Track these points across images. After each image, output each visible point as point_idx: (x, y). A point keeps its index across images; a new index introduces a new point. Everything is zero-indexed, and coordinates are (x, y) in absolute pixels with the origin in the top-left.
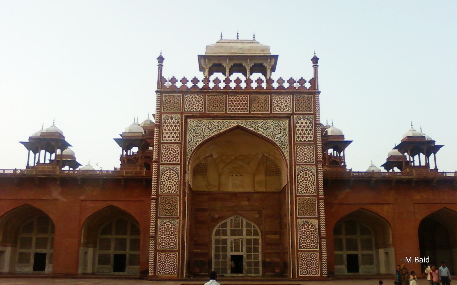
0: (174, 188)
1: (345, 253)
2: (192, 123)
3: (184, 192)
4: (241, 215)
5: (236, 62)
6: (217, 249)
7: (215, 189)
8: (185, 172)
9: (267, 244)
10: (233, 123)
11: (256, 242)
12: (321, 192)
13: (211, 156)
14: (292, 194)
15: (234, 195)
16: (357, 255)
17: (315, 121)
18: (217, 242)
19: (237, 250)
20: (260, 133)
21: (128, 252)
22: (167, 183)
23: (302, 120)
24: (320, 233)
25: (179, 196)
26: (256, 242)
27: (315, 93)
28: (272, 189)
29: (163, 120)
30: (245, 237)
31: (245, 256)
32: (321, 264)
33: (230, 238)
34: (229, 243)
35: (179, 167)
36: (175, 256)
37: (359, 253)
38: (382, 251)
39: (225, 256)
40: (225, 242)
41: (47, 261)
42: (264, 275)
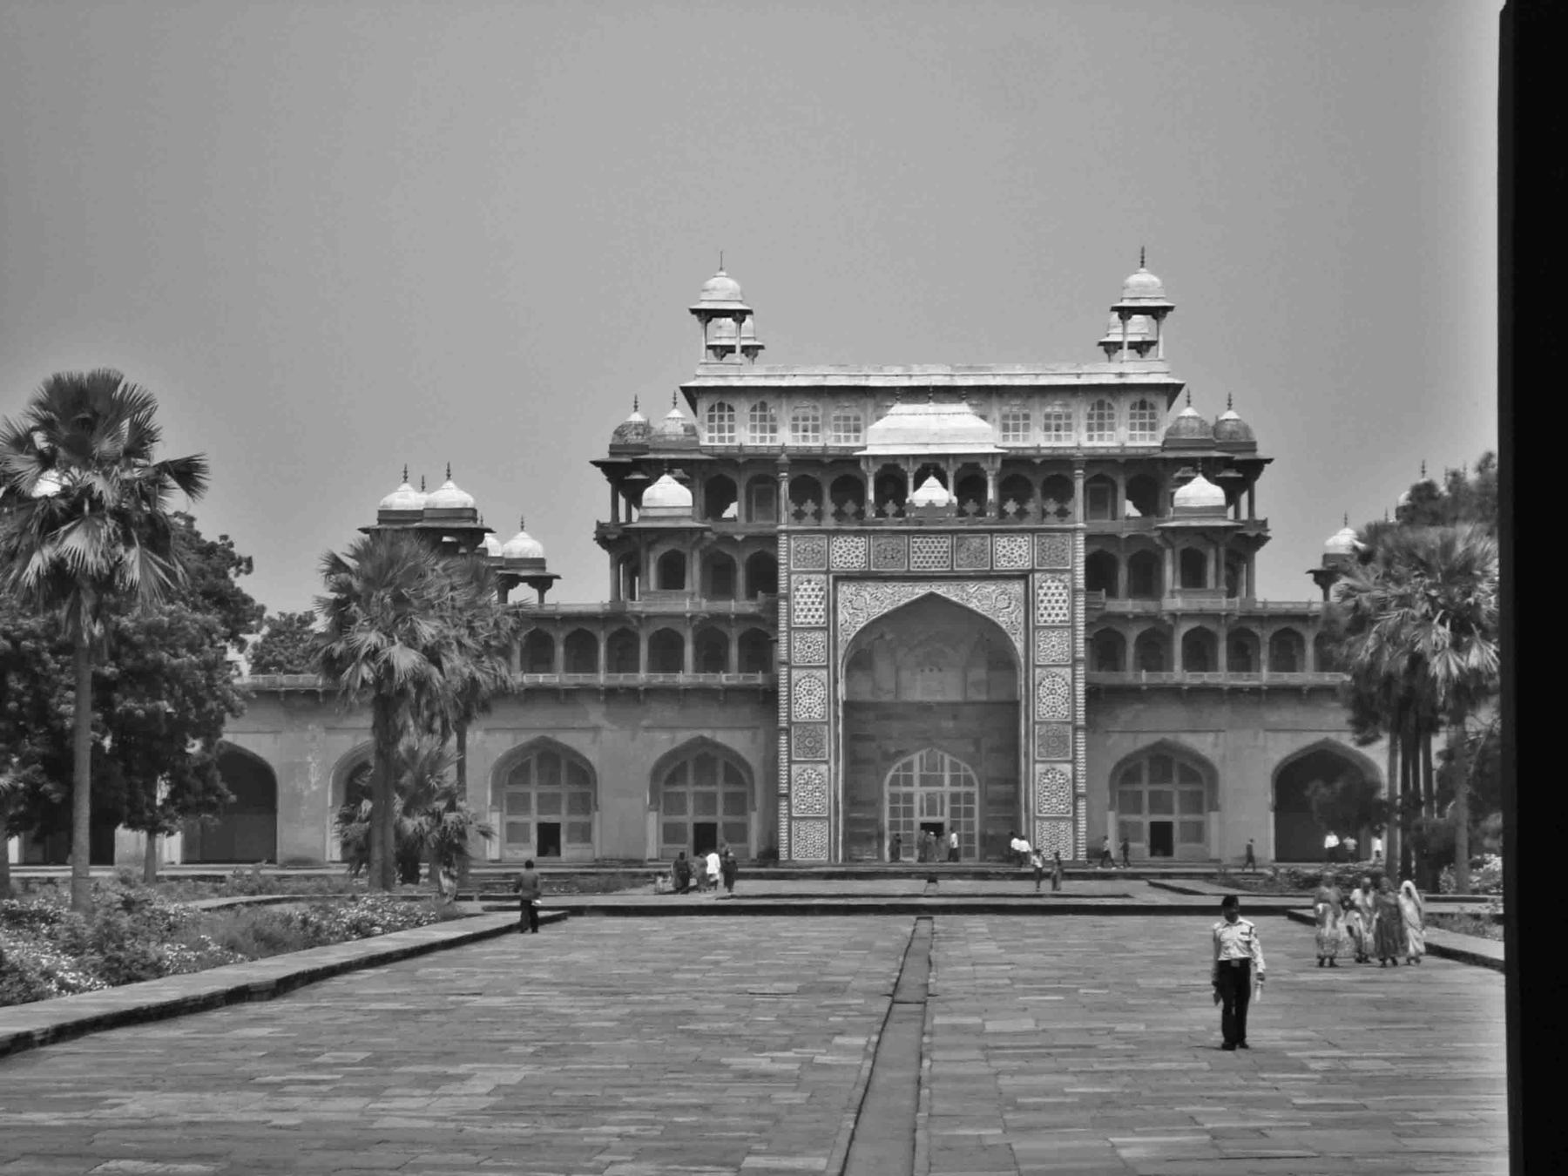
0: (818, 710)
1: (1146, 819)
2: (846, 590)
3: (836, 716)
4: (940, 748)
5: (928, 461)
6: (894, 811)
7: (887, 698)
8: (836, 681)
9: (988, 802)
10: (921, 590)
11: (969, 798)
12: (1081, 714)
13: (882, 636)
14: (1027, 719)
15: (925, 708)
16: (1167, 827)
17: (1074, 584)
18: (895, 798)
19: (931, 812)
20: (971, 606)
21: (720, 818)
22: (805, 701)
23: (1049, 583)
24: (1075, 787)
25: (828, 723)
26: (969, 798)
27: (1075, 530)
28: (1001, 695)
29: (793, 586)
30: (947, 788)
31: (947, 826)
32: (1076, 840)
33: (918, 791)
34: (917, 799)
35: (825, 672)
36: (823, 827)
37: (1175, 818)
38: (1214, 816)
39: (909, 825)
40: (909, 798)
41: (563, 838)
42: (983, 858)
